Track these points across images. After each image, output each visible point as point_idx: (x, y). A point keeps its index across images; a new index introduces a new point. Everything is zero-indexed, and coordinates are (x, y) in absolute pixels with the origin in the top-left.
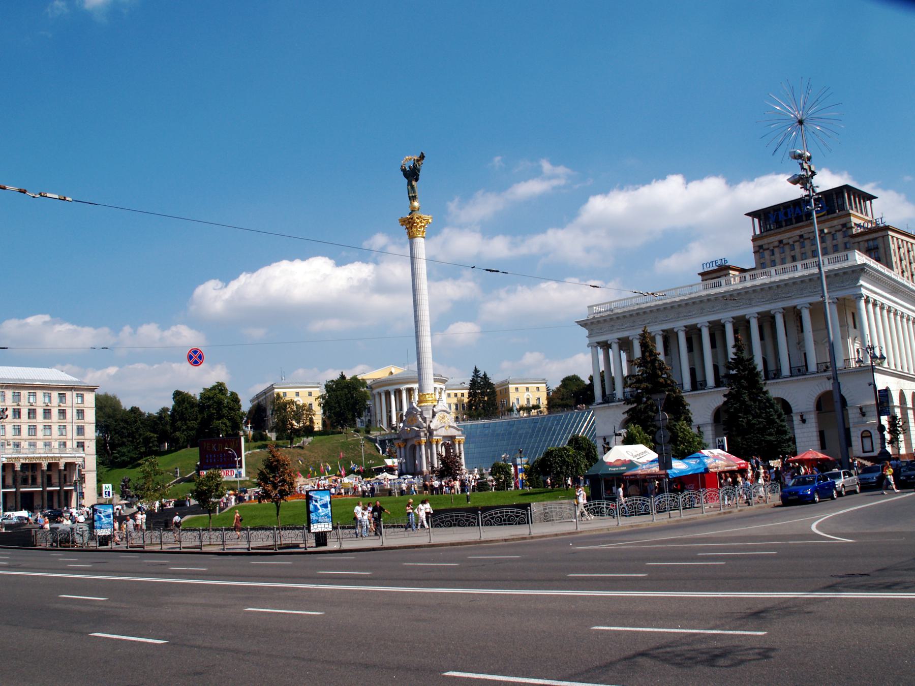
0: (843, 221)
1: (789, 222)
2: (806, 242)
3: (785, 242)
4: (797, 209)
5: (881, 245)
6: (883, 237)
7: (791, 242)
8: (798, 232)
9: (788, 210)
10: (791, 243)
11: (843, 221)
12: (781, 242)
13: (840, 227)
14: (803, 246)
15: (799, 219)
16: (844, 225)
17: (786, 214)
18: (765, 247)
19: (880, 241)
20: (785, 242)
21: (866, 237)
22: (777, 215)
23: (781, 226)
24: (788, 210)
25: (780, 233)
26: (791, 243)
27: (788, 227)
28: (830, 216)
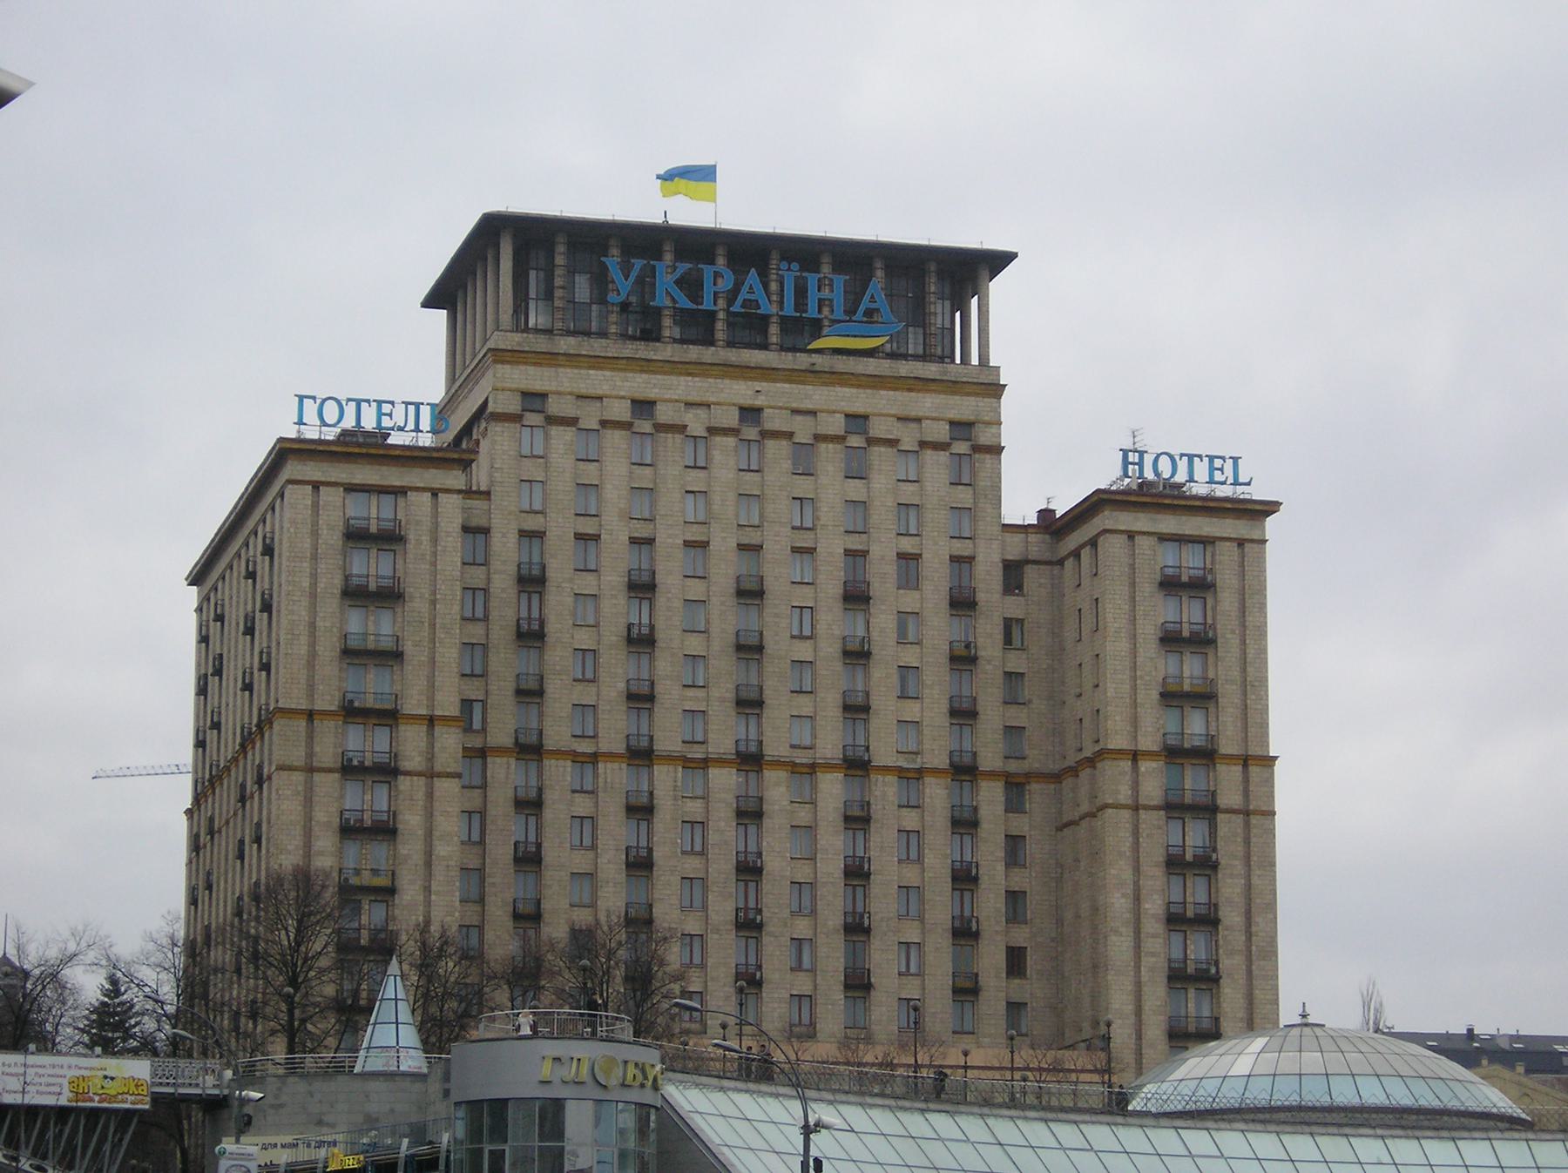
0: (963, 407)
1: (698, 327)
2: (770, 444)
3: (664, 414)
4: (753, 277)
5: (1226, 578)
6: (1241, 543)
7: (696, 423)
8: (742, 391)
9: (708, 271)
10: (696, 428)
11: (963, 407)
12: (644, 406)
13: (941, 432)
14: (857, 473)
15: (750, 329)
16: (962, 428)
17: (691, 285)
18: (555, 407)
19: (1226, 555)
20: (664, 414)
21: (1169, 524)
22: (645, 283)
23: (650, 335)
24: (708, 271)
25: (646, 366)
26: (803, 437)
27: (694, 352)
28: (905, 368)
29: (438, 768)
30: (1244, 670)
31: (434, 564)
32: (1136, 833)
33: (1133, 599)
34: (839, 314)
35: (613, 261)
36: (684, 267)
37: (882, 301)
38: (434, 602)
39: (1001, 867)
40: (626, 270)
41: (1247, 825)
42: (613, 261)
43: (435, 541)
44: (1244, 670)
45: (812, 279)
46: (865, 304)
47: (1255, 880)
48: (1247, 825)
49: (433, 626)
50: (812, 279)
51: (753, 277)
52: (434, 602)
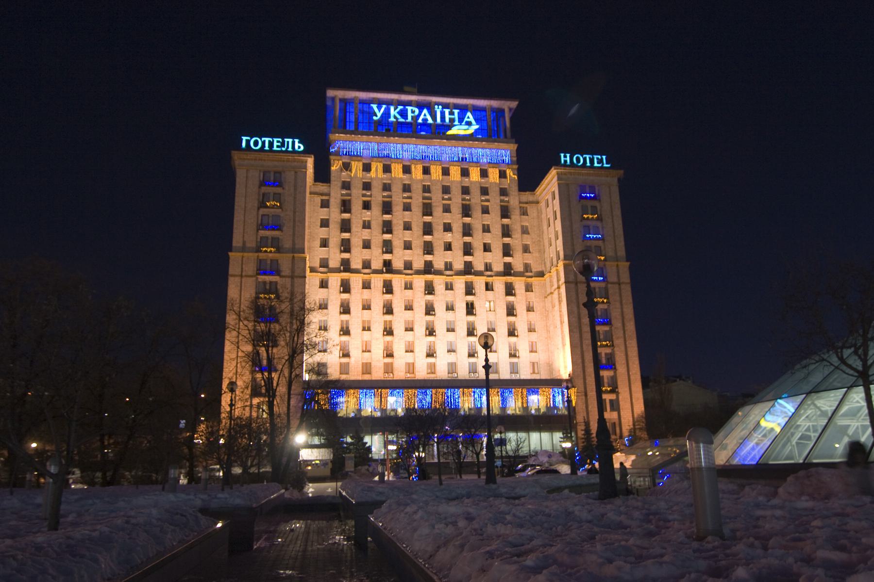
4: (425, 111)
9: (409, 108)
29: (296, 274)
30: (614, 232)
31: (295, 198)
32: (577, 291)
33: (569, 207)
34: (456, 123)
35: (375, 106)
36: (400, 107)
37: (472, 119)
38: (295, 212)
39: (525, 311)
40: (379, 108)
41: (620, 289)
42: (375, 106)
43: (295, 189)
44: (614, 232)
45: (447, 111)
46: (466, 119)
47: (625, 310)
48: (620, 289)
49: (294, 221)
50: (447, 111)
51: (425, 111)
52: (295, 212)
